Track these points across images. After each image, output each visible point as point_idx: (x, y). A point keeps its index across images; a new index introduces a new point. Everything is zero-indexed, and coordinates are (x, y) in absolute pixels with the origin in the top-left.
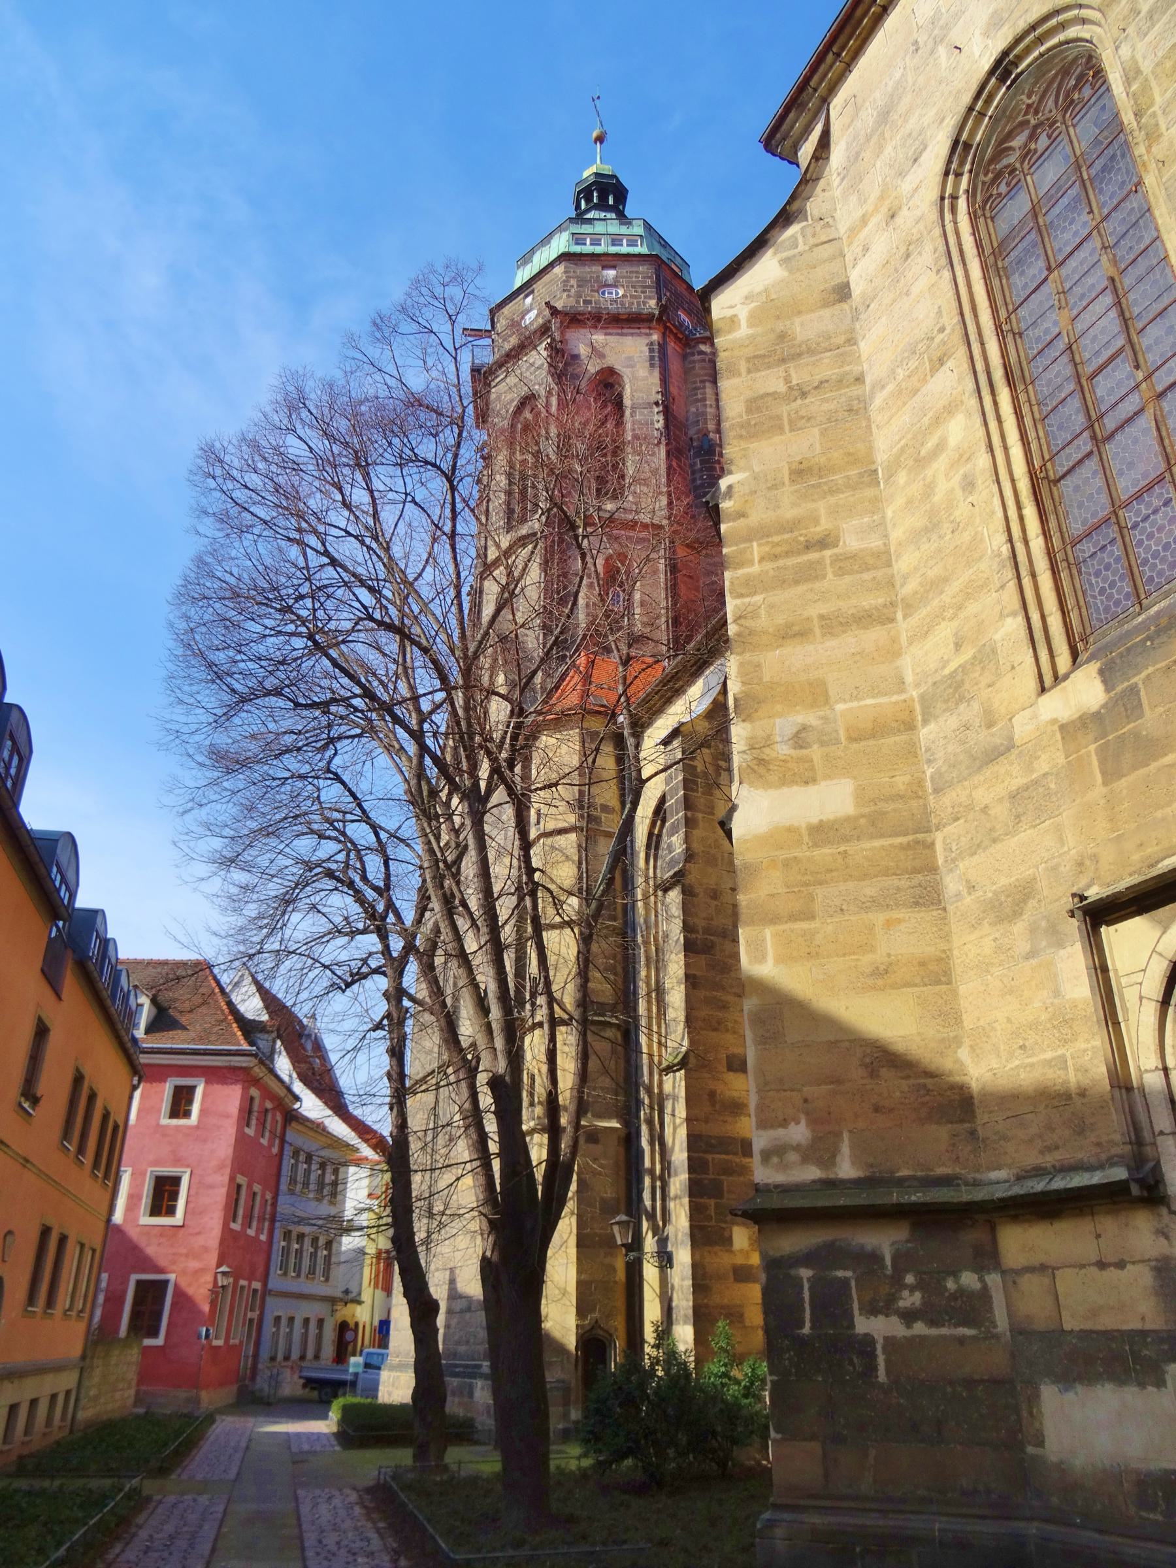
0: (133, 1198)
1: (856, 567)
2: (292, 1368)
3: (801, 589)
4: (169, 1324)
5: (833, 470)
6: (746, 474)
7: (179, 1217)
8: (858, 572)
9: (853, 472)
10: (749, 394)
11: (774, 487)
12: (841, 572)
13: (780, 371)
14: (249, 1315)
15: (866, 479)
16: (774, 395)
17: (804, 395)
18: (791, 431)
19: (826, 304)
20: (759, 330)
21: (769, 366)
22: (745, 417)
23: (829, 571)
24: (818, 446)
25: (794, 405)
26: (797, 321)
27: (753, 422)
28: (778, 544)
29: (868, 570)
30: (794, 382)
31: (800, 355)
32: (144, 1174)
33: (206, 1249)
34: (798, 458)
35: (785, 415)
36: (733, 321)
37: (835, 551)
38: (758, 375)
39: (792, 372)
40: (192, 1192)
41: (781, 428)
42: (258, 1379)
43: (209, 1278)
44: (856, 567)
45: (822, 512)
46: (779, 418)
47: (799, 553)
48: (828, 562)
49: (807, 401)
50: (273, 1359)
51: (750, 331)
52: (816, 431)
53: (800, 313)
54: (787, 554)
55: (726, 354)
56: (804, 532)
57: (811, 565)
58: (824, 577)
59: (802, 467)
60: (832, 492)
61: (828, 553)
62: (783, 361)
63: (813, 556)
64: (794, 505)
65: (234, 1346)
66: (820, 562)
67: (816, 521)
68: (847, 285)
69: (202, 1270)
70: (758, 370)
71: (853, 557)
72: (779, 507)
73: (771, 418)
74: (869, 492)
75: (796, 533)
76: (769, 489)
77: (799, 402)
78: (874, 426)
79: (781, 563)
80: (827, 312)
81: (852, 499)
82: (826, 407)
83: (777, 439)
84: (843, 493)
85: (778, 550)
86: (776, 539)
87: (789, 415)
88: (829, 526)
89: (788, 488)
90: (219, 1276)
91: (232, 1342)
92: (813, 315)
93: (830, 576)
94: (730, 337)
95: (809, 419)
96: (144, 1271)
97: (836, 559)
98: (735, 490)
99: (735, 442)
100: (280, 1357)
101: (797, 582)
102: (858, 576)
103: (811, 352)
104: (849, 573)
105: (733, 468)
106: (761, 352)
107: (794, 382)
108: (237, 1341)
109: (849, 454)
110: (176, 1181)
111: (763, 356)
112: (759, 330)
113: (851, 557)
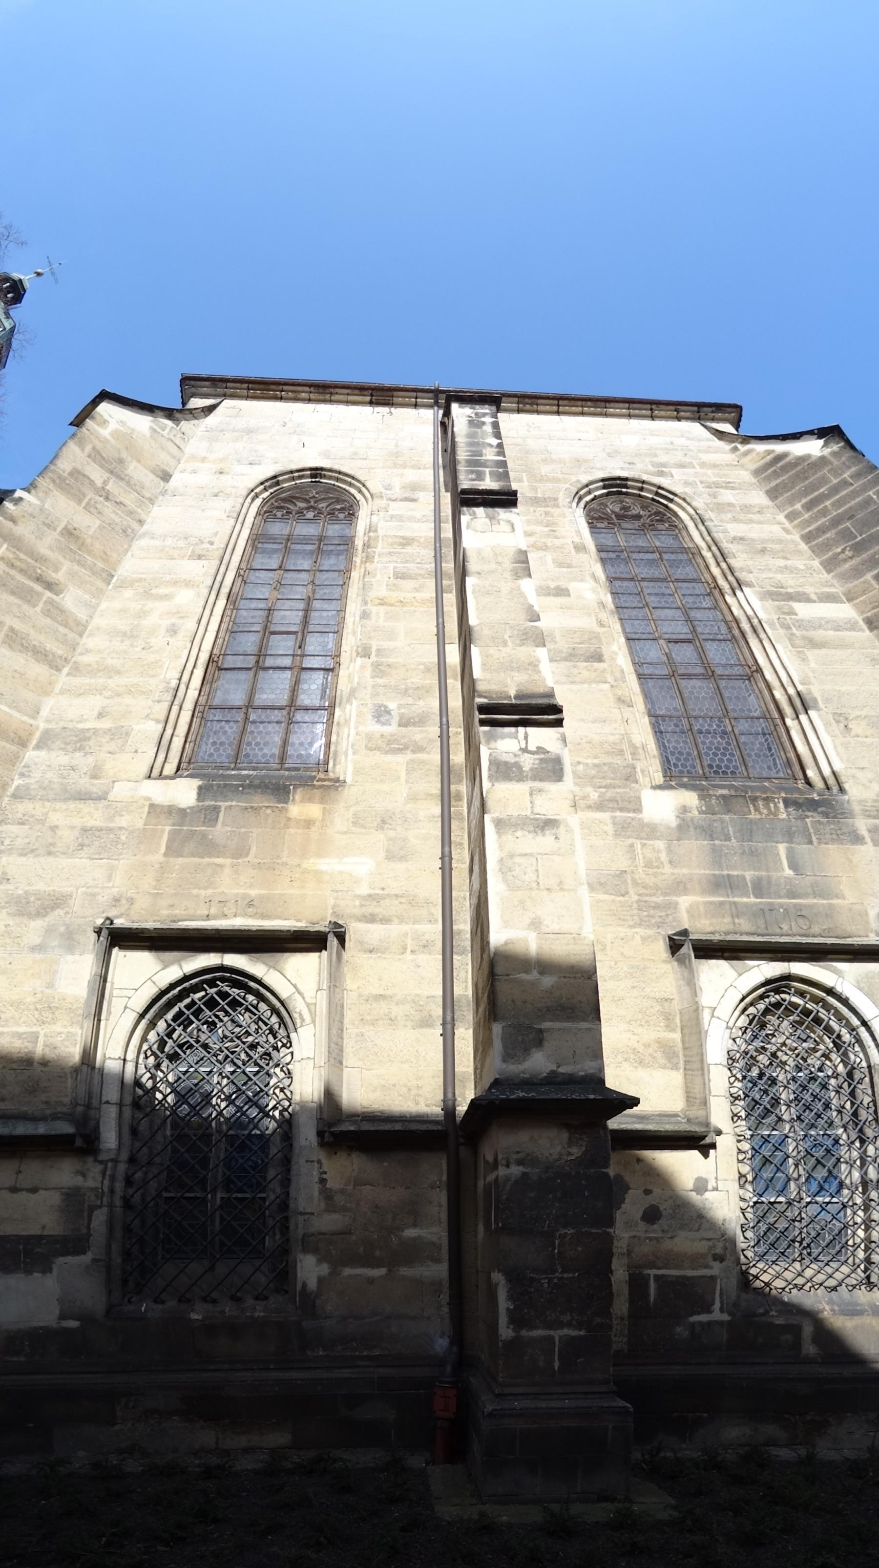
1: (60, 619)
3: (12, 599)
5: (90, 552)
6: (38, 503)
8: (58, 622)
9: (100, 565)
10: (79, 467)
11: (48, 526)
12: (47, 613)
13: (106, 475)
15: (104, 575)
16: (92, 483)
17: (107, 499)
18: (84, 508)
19: (153, 472)
20: (113, 441)
21: (102, 466)
22: (66, 475)
23: (41, 605)
24: (92, 530)
25: (97, 498)
26: (135, 463)
27: (67, 482)
28: (20, 560)
29: (66, 626)
30: (108, 488)
31: (122, 479)
34: (75, 525)
35: (89, 497)
36: (105, 423)
37: (54, 597)
38: (93, 464)
39: (111, 482)
41: (80, 501)
44: (60, 619)
45: (65, 568)
46: (84, 495)
47: (30, 577)
48: (44, 599)
49: (106, 503)
51: (108, 437)
52: (98, 522)
53: (139, 461)
54: (21, 571)
55: (86, 432)
56: (44, 568)
57: (31, 590)
58: (34, 606)
59: (74, 532)
60: (79, 563)
61: (48, 594)
62: (112, 472)
63: (38, 588)
64: (50, 548)
66: (39, 595)
67: (57, 570)
68: (171, 476)
70: (94, 461)
71: (62, 611)
72: (41, 539)
73: (80, 490)
74: (100, 584)
75: (37, 565)
76: (44, 523)
77: (102, 499)
78: (129, 554)
79: (13, 572)
80: (152, 476)
81: (87, 578)
82: (113, 516)
83: (73, 504)
84: (85, 569)
85: (18, 563)
86: (22, 556)
87: (90, 499)
88: (62, 580)
89: (56, 535)
92: (144, 470)
93: (38, 609)
94: (96, 426)
95: (99, 513)
97: (50, 602)
98: (24, 504)
99: (48, 480)
101: (13, 593)
102: (56, 625)
103: (128, 483)
104: (52, 619)
105: (33, 491)
106: (104, 455)
107: (108, 488)
109: (105, 553)
111: (104, 459)
112: (113, 441)
113: (61, 611)
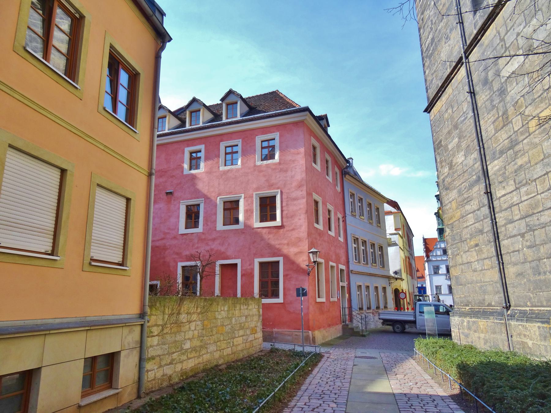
0: (248, 212)
2: (373, 313)
4: (284, 289)
7: (278, 221)
14: (341, 284)
32: (252, 197)
33: (300, 240)
40: (284, 204)
42: (354, 321)
43: (305, 257)
50: (361, 309)
65: (334, 302)
69: (301, 253)
90: (311, 255)
91: (332, 300)
96: (262, 256)
100: (365, 308)
108: (336, 299)
110: (273, 199)
